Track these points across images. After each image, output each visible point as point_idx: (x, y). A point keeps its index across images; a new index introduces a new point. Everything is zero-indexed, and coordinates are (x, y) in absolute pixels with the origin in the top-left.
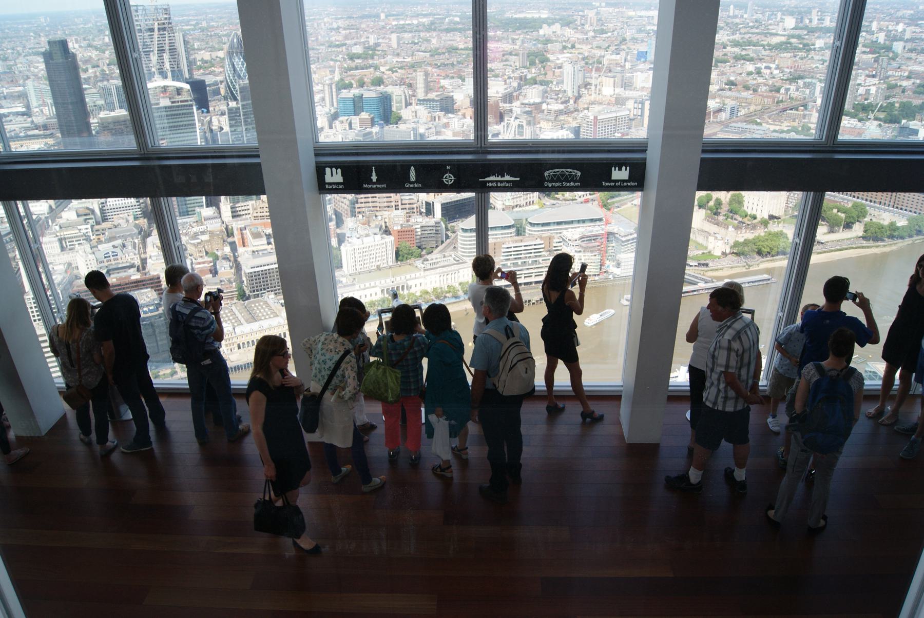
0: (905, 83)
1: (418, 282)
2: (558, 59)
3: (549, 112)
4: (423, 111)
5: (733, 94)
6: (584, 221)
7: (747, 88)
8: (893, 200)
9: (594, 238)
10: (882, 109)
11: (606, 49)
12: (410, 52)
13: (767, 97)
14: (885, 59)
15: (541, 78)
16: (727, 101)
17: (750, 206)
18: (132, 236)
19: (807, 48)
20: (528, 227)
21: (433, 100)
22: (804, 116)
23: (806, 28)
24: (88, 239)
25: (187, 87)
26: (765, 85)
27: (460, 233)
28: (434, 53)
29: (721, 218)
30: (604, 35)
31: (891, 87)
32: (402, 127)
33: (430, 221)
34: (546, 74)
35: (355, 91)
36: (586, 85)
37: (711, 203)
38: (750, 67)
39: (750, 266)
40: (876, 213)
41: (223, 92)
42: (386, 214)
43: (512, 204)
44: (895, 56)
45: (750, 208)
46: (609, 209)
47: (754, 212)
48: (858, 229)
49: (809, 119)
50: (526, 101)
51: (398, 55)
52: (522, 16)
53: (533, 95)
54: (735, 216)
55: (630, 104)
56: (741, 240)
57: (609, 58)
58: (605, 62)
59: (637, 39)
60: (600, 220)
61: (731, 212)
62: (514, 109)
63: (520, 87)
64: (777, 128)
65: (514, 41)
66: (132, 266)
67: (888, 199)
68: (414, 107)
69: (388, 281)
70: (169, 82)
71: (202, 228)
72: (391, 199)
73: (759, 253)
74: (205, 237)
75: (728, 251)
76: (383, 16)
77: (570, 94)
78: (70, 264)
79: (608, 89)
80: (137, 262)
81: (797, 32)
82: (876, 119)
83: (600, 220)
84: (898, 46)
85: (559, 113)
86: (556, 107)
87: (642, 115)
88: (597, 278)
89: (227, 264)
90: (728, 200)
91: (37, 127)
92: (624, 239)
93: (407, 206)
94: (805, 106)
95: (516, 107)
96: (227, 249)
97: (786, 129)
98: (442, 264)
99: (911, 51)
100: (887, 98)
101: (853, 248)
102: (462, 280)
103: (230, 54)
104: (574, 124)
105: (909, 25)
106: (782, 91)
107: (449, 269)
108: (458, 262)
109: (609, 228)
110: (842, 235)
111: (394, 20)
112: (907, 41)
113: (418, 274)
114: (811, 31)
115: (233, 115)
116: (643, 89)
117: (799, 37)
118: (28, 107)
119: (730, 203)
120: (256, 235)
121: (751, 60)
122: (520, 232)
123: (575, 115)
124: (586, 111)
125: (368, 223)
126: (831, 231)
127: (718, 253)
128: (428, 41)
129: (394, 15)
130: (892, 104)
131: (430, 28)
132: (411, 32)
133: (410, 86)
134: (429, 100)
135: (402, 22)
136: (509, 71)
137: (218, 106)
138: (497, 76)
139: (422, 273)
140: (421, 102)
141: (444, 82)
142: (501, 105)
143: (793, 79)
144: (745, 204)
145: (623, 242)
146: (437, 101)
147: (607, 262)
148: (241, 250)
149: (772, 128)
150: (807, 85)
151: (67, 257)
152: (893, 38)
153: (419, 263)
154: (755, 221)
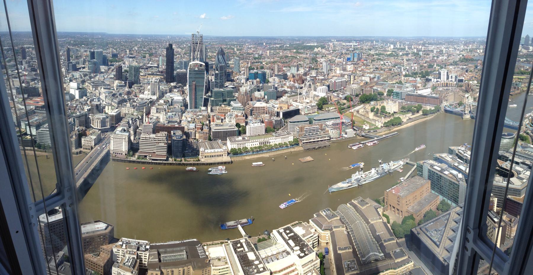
1: (273, 141)
3: (319, 79)
4: (277, 79)
5: (378, 72)
6: (333, 118)
7: (382, 70)
9: (338, 124)
10: (420, 74)
11: (336, 57)
15: (316, 67)
18: (178, 112)
19: (397, 55)
20: (314, 121)
24: (165, 110)
25: (204, 64)
27: (289, 123)
28: (281, 58)
29: (379, 114)
33: (279, 119)
35: (255, 71)
36: (331, 70)
37: (375, 110)
38: (382, 63)
41: (214, 67)
42: (263, 115)
44: (421, 56)
53: (313, 73)
55: (346, 77)
57: (338, 60)
58: (336, 62)
60: (339, 118)
63: (309, 70)
66: (176, 122)
68: (273, 77)
70: (199, 62)
71: (201, 113)
74: (201, 117)
76: (264, 44)
77: (325, 73)
78: (158, 117)
79: (338, 71)
80: (178, 121)
83: (339, 118)
84: (421, 53)
85: (323, 80)
87: (350, 80)
89: (206, 127)
91: (159, 72)
95: (308, 78)
96: (208, 122)
99: (425, 54)
102: (289, 140)
103: (218, 54)
104: (328, 84)
108: (289, 134)
109: (342, 121)
115: (216, 75)
116: (350, 71)
117: (394, 52)
118: (158, 65)
119: (381, 109)
120: (218, 119)
121: (382, 60)
122: (311, 123)
125: (256, 118)
130: (423, 72)
136: (305, 65)
137: (212, 72)
140: (276, 75)
141: (284, 69)
148: (212, 123)
150: (399, 68)
151: (157, 115)
152: (419, 50)
153: (274, 134)
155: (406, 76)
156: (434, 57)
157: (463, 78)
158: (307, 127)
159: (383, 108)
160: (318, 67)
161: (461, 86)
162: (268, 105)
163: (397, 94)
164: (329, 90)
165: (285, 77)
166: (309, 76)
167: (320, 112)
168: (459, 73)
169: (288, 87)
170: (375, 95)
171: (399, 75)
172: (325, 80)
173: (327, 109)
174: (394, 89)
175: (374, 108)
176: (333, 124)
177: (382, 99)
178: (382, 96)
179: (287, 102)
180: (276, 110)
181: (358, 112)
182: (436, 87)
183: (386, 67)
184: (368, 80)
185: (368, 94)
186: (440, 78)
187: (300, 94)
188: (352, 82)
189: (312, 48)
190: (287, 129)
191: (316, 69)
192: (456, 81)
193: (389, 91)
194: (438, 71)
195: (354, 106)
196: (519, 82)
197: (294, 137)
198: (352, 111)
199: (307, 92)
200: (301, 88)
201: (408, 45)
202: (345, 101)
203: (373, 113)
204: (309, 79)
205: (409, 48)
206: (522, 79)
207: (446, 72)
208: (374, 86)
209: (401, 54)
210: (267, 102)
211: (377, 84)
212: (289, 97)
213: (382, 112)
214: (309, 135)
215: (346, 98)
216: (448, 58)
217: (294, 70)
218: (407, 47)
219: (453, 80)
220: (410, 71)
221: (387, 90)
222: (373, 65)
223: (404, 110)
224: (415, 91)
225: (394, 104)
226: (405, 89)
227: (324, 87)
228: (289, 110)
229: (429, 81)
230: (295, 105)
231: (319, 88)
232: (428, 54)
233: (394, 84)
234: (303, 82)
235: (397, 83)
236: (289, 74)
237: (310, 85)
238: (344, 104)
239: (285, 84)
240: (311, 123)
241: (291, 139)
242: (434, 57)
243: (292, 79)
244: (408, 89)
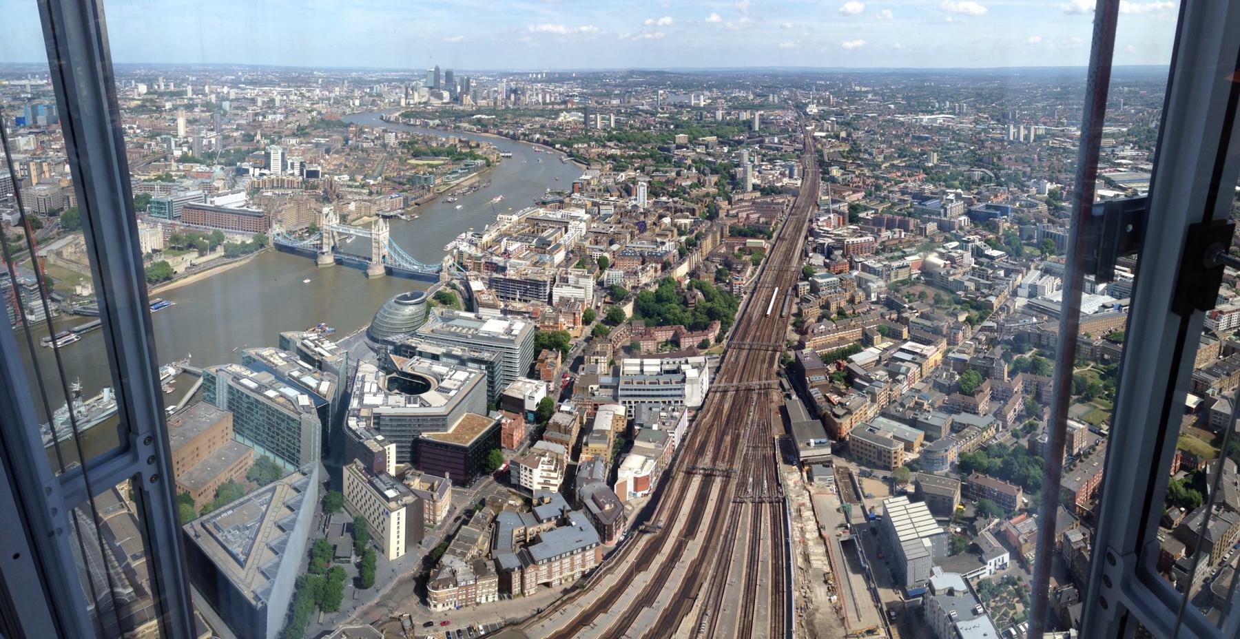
0: (235, 134)
10: (222, 156)
19: (159, 109)
22: (166, 166)
23: (155, 93)
31: (226, 138)
44: (226, 112)
81: (150, 97)
82: (219, 164)
84: (226, 105)
87: (30, 175)
94: (166, 159)
99: (237, 108)
100: (224, 146)
105: (231, 88)
114: (161, 95)
117: (151, 100)
130: (228, 151)
143: (152, 136)
149: (143, 178)
150: (164, 141)
155: (184, 159)
156: (257, 114)
157: (319, 168)
161: (314, 187)
168: (309, 156)
171: (166, 159)
174: (152, 193)
182: (258, 189)
186: (267, 166)
188: (35, 181)
192: (302, 174)
194: (264, 149)
196: (430, 173)
201: (193, 84)
205: (194, 92)
206: (436, 166)
207: (280, 152)
209: (168, 105)
216: (286, 118)
218: (189, 89)
219: (297, 172)
220: (195, 148)
226: (182, 194)
229: (242, 175)
232: (245, 109)
233: (151, 180)
235: (159, 178)
242: (257, 114)
244: (191, 192)
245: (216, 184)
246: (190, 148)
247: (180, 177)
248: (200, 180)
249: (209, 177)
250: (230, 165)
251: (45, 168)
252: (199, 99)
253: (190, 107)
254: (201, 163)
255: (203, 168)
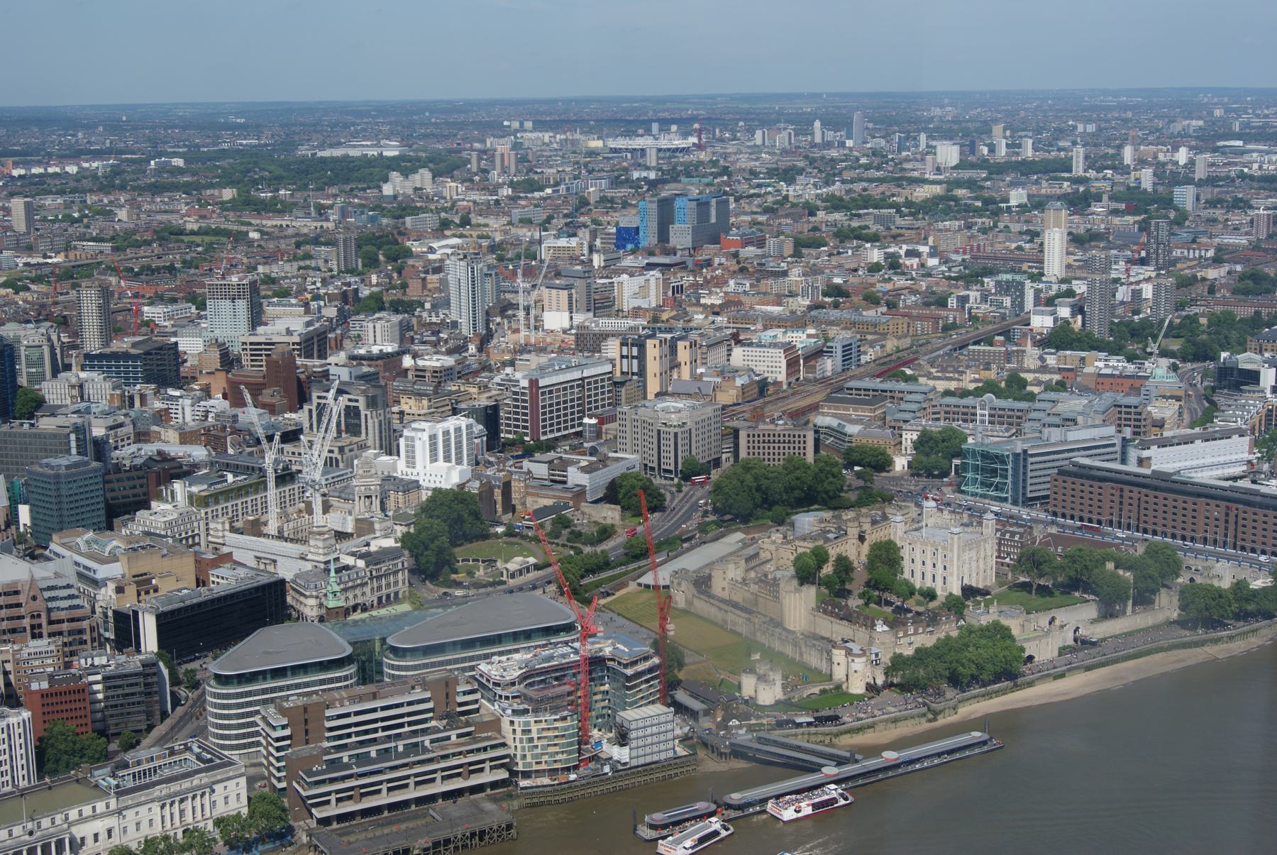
0: (1212, 274)
1: (100, 826)
2: (432, 251)
3: (420, 373)
4: (99, 385)
5: (846, 315)
6: (528, 635)
7: (872, 300)
8: (1231, 533)
9: (560, 673)
10: (1173, 332)
11: (544, 225)
12: (59, 241)
13: (920, 318)
14: (1163, 223)
15: (395, 294)
16: (832, 331)
17: (918, 568)
21: (126, 356)
22: (1008, 356)
26: (913, 292)
27: (212, 688)
28: (124, 241)
29: (854, 603)
30: (537, 194)
31: (1187, 283)
32: (46, 424)
33: (133, 663)
34: (404, 286)
37: (828, 569)
38: (875, 255)
39: (936, 714)
40: (1199, 564)
43: (341, 603)
45: (918, 576)
46: (587, 602)
47: (929, 583)
48: (1167, 607)
49: (1021, 362)
50: (362, 352)
51: (30, 249)
52: (337, 153)
53: (378, 336)
54: (886, 595)
55: (612, 348)
56: (909, 652)
57: (553, 244)
58: (545, 255)
59: (612, 201)
60: (569, 628)
61: (876, 587)
62: (333, 370)
63: (343, 317)
64: (953, 385)
65: (321, 211)
67: (1221, 530)
69: (17, 830)
72: (22, 611)
73: (955, 680)
75: (880, 681)
77: (466, 330)
81: (966, 174)
82: (1164, 353)
83: (569, 628)
85: (443, 375)
86: (434, 361)
87: (642, 372)
88: (573, 777)
90: (864, 559)
92: (629, 672)
93: (65, 627)
94: (1007, 333)
97: (972, 386)
98: (167, 773)
100: (1180, 306)
101: (1161, 650)
102: (221, 810)
104: (483, 401)
106: (952, 302)
107: (186, 784)
109: (591, 648)
110: (1131, 621)
111: (16, 165)
112: (1200, 184)
113: (101, 807)
116: (636, 312)
121: (874, 239)
123: (483, 378)
124: (509, 370)
126: (1108, 613)
127: (857, 688)
128: (108, 214)
129: (15, 154)
130: (1193, 319)
131: (108, 184)
132: (61, 193)
133: (63, 323)
134: (115, 356)
135: (36, 170)
138: (285, 294)
139: (113, 803)
140: (91, 361)
142: (299, 361)
143: (972, 276)
144: (906, 564)
145: (629, 679)
146: (134, 358)
147: (595, 733)
149: (941, 386)
150: (1004, 288)
153: (103, 777)
154: (932, 605)
155: (1059, 339)
158: (345, 704)
159: (887, 556)
160: (414, 292)
162: (43, 572)
163: (991, 464)
164: (493, 440)
165: (164, 367)
166: (342, 356)
167: (431, 591)
169: (187, 437)
170: (825, 470)
171: (1007, 333)
172: (462, 373)
173: (480, 573)
174: (967, 428)
175: (820, 557)
176: (528, 676)
177: (875, 498)
178: (879, 479)
179: (190, 542)
180: (107, 596)
181: (702, 583)
183: (900, 282)
184: (774, 366)
185: (775, 460)
187: (286, 477)
188: (653, 386)
189: (379, 169)
190: (201, 732)
191: (396, 307)
193: (925, 442)
195: (674, 544)
197: (251, 781)
198: (663, 576)
199: (330, 463)
200: (291, 436)
202: (610, 514)
203: (810, 592)
204: (345, 374)
205: (1091, 163)
208: (814, 408)
209: (1017, 197)
210: (34, 550)
211: (837, 392)
212: (203, 501)
213: (875, 587)
214: (362, 759)
215: (612, 494)
217: (227, 322)
220: (1094, 310)
221: (910, 437)
222: (814, 271)
223: (1043, 577)
224: (1133, 454)
225: (970, 534)
226: (1055, 435)
227: (462, 422)
228: (204, 594)
230: (247, 557)
231: (419, 435)
232: (1242, 205)
233: (964, 393)
234: (301, 398)
235: (990, 387)
236: (191, 345)
237: (352, 412)
238: (606, 532)
239: (162, 417)
240: (366, 665)
241: (232, 797)
243: (219, 383)
245: (1156, 410)
246: (1078, 309)
247: (1049, 387)
248: (1108, 397)
249: (1135, 390)
250: (1197, 358)
251: (683, 354)
252: (1102, 182)
253: (1079, 202)
254: (1114, 350)
255: (1117, 364)
